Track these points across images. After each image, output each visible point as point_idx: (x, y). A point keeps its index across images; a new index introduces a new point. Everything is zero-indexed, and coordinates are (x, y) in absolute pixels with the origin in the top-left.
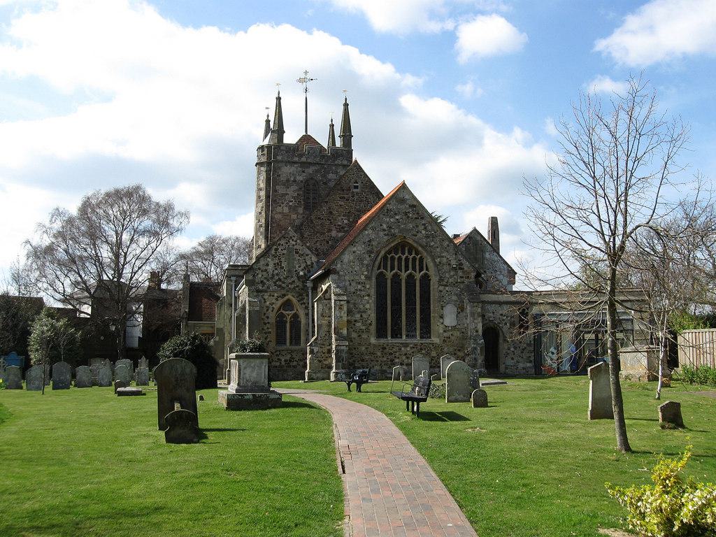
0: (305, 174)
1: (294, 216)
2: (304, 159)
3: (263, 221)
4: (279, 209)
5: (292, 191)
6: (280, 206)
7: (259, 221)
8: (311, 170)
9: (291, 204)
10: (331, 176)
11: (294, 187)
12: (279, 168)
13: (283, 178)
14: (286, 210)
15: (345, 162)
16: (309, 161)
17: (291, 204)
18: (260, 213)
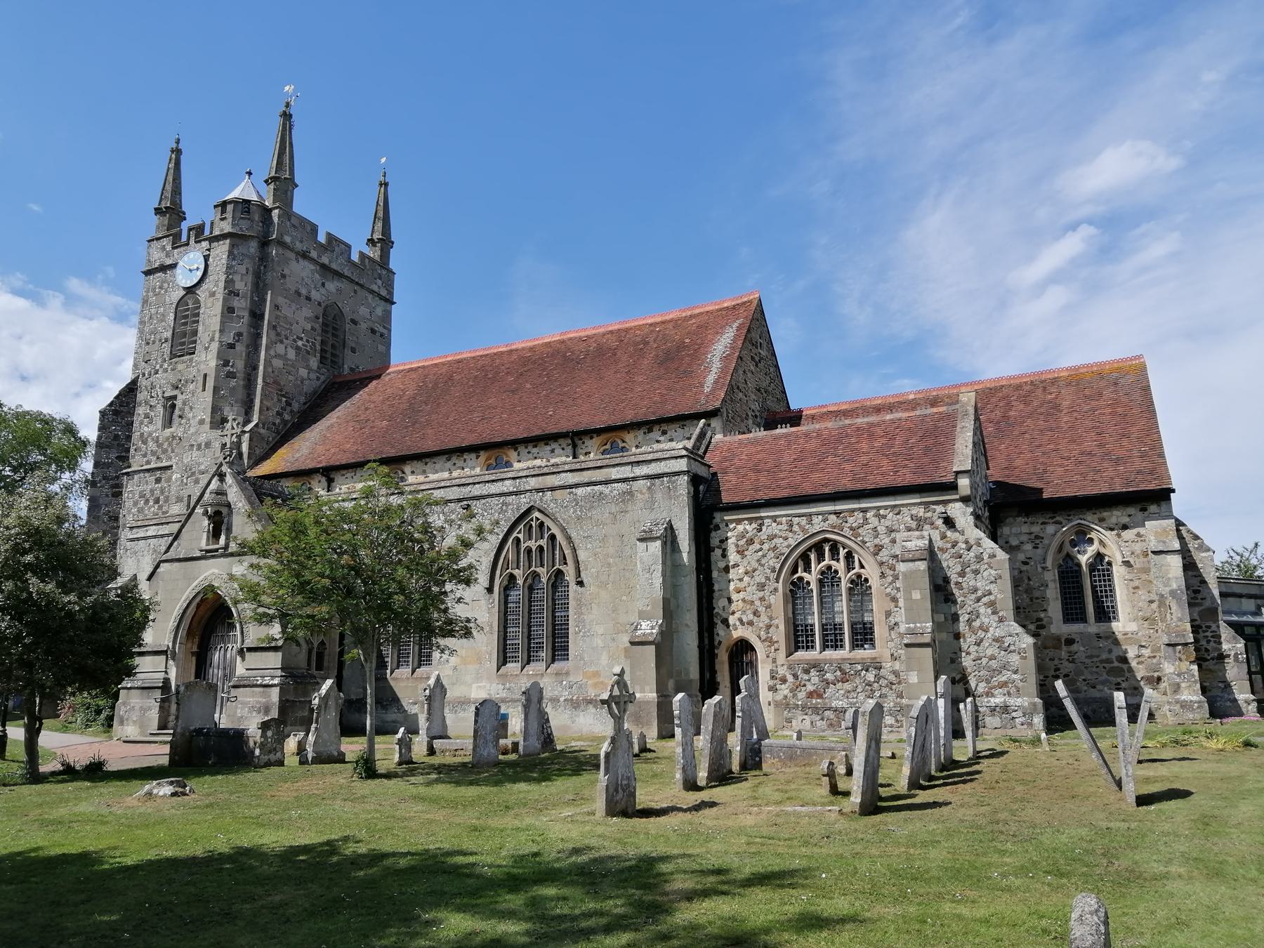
0: (323, 291)
1: (303, 372)
2: (325, 260)
3: (240, 364)
4: (280, 348)
5: (302, 318)
6: (281, 342)
7: (226, 363)
8: (332, 286)
9: (300, 343)
10: (363, 311)
11: (307, 312)
12: (287, 261)
13: (291, 284)
14: (292, 354)
15: (384, 293)
16: (334, 266)
17: (300, 343)
18: (232, 346)
